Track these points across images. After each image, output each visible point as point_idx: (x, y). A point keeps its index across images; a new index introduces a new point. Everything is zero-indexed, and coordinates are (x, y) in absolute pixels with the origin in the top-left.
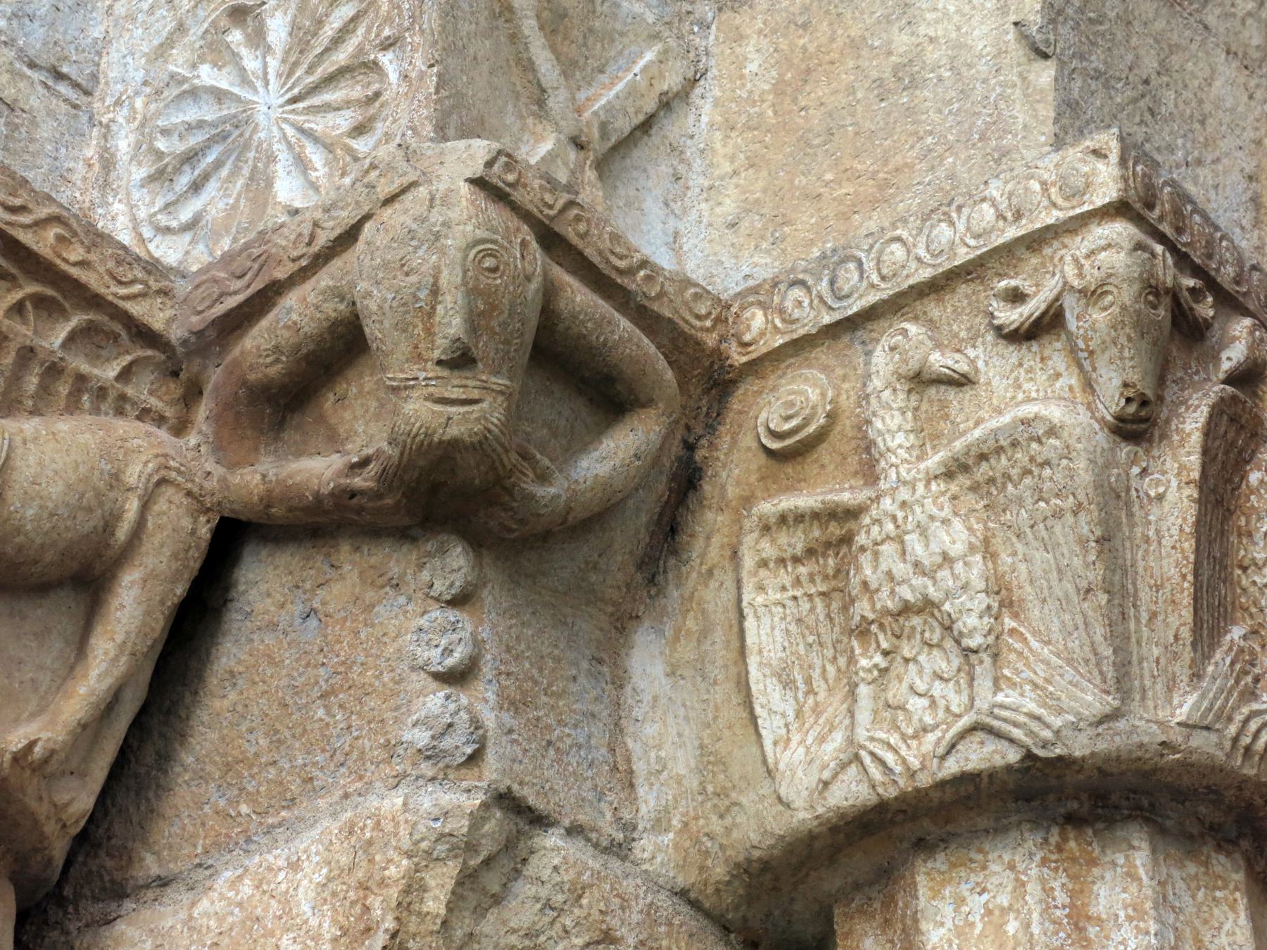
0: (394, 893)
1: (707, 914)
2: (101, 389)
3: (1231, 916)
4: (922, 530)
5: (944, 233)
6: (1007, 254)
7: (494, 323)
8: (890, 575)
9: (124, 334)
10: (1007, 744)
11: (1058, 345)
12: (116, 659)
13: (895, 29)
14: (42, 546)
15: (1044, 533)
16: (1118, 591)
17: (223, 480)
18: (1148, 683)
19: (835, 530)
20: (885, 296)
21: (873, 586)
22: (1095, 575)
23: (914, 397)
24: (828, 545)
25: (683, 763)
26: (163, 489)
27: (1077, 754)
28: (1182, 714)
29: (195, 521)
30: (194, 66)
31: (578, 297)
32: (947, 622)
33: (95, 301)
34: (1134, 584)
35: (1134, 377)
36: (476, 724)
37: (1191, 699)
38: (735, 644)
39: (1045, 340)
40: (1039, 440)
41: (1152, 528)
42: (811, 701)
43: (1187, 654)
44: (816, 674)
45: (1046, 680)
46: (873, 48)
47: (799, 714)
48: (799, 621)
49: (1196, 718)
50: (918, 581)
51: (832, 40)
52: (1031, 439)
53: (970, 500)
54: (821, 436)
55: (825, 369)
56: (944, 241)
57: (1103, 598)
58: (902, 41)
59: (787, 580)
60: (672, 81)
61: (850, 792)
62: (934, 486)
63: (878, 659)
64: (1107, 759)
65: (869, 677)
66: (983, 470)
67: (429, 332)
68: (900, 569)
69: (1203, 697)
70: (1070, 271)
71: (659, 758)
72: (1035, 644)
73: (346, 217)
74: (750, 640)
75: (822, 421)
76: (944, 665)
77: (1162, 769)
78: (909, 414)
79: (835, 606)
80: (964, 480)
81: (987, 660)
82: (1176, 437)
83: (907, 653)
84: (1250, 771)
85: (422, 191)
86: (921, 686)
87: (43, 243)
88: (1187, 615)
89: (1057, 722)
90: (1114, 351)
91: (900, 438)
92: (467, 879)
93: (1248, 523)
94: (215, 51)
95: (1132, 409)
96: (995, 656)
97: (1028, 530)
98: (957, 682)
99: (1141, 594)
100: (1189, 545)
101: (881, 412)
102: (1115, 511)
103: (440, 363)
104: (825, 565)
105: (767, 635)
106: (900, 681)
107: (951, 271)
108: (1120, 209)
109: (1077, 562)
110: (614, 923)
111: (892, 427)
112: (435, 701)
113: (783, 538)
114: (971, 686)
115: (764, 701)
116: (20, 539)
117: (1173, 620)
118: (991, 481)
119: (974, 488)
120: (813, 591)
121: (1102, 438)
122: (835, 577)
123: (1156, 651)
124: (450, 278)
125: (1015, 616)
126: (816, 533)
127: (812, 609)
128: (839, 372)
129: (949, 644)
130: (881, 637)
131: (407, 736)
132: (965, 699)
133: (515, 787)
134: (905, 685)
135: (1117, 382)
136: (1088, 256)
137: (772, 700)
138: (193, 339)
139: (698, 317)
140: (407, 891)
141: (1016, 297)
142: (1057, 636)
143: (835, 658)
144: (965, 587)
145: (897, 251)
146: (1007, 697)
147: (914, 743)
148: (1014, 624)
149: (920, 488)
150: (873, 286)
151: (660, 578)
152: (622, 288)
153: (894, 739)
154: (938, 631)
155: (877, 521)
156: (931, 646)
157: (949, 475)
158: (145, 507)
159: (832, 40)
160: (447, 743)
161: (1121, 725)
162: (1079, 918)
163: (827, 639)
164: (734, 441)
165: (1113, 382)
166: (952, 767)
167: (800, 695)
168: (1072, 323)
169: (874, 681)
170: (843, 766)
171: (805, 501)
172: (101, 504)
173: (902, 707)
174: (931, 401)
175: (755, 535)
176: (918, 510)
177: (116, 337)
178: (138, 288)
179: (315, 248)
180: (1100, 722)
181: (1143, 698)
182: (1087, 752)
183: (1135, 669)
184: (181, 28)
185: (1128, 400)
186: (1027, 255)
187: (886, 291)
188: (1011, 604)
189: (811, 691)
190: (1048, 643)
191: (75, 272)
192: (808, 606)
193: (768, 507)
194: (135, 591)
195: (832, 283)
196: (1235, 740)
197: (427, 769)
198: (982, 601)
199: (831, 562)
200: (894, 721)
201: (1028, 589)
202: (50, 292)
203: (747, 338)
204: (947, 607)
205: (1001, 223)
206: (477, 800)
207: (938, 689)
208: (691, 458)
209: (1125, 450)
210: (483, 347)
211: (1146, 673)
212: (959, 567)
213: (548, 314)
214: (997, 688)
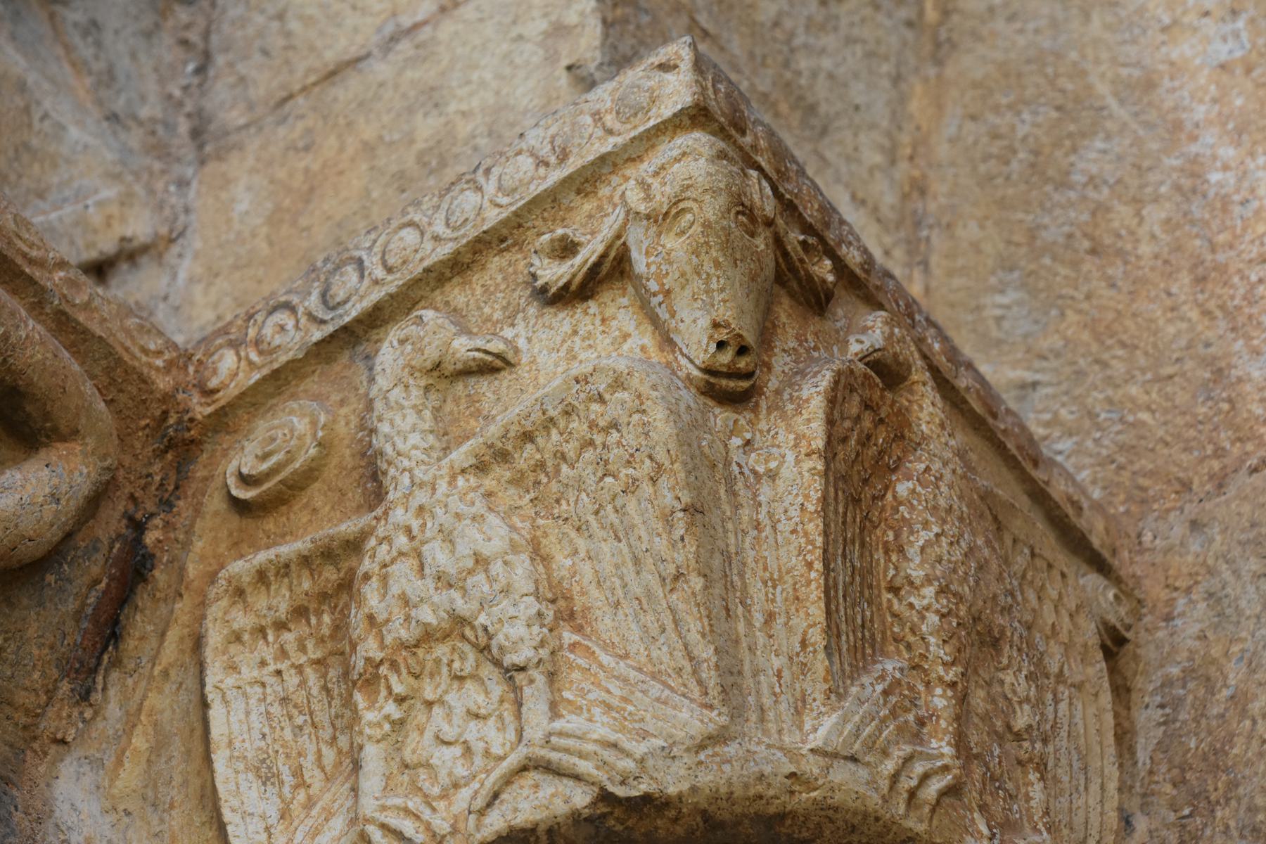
4: (448, 537)
5: (469, 200)
6: (550, 202)
8: (405, 601)
10: (571, 783)
11: (624, 301)
13: (419, 116)
15: (613, 517)
16: (721, 582)
18: (767, 701)
19: (330, 575)
20: (392, 289)
21: (381, 618)
22: (685, 555)
23: (433, 396)
24: (324, 597)
27: (672, 790)
28: (816, 740)
32: (483, 640)
34: (741, 575)
35: (725, 313)
37: (829, 722)
38: (198, 748)
39: (606, 296)
40: (601, 399)
41: (764, 510)
42: (301, 796)
43: (820, 663)
44: (308, 762)
45: (625, 700)
46: (391, 143)
47: (284, 815)
48: (285, 700)
49: (837, 743)
50: (442, 598)
51: (342, 149)
52: (591, 400)
53: (510, 496)
54: (310, 474)
55: (317, 397)
56: (468, 207)
57: (697, 583)
58: (426, 127)
59: (267, 652)
60: (140, 227)
62: (461, 482)
63: (391, 709)
64: (715, 798)
65: (378, 733)
69: (845, 720)
70: (634, 197)
72: (605, 659)
74: (216, 731)
75: (313, 451)
76: (481, 699)
77: (793, 814)
78: (427, 414)
79: (333, 674)
80: (502, 472)
81: (540, 679)
82: (790, 407)
83: (429, 694)
84: (916, 825)
86: (449, 732)
88: (817, 611)
89: (640, 749)
90: (698, 284)
91: (415, 439)
93: (897, 537)
95: (726, 357)
96: (552, 676)
97: (591, 518)
98: (501, 717)
99: (751, 590)
100: (814, 528)
101: (390, 415)
102: (712, 500)
104: (319, 623)
105: (237, 722)
106: (421, 731)
107: (478, 240)
109: (661, 544)
111: (405, 429)
113: (260, 601)
114: (518, 715)
115: (235, 803)
117: (799, 622)
118: (541, 466)
119: (518, 481)
120: (303, 659)
121: (688, 397)
122: (332, 637)
123: (777, 663)
125: (579, 629)
126: (306, 585)
127: (303, 684)
128: (335, 397)
129: (487, 670)
130: (394, 679)
132: (511, 735)
134: (429, 735)
135: (704, 322)
136: (656, 174)
139: (145, 351)
141: (566, 249)
142: (637, 647)
143: (334, 738)
144: (506, 591)
145: (410, 236)
147: (441, 805)
148: (576, 638)
149: (443, 486)
150: (376, 282)
151: (96, 697)
152: (31, 281)
153: (414, 803)
154: (471, 656)
155: (387, 539)
156: (461, 679)
157: (481, 468)
159: (342, 149)
161: (731, 749)
163: (322, 717)
164: (198, 511)
167: (286, 790)
168: (640, 262)
169: (385, 737)
171: (288, 550)
173: (428, 765)
174: (457, 401)
175: (224, 603)
176: (439, 511)
180: (701, 747)
181: (762, 720)
182: (685, 786)
183: (749, 682)
185: (721, 345)
186: (577, 201)
187: (393, 283)
188: (572, 615)
190: (626, 656)
192: (296, 680)
193: (240, 568)
195: (324, 296)
196: (895, 778)
198: (530, 606)
199: (326, 618)
200: (413, 782)
201: (594, 592)
203: (213, 383)
204: (482, 619)
205: (542, 171)
207: (473, 731)
208: (138, 541)
209: (721, 417)
211: (765, 691)
212: (497, 568)
214: (554, 710)
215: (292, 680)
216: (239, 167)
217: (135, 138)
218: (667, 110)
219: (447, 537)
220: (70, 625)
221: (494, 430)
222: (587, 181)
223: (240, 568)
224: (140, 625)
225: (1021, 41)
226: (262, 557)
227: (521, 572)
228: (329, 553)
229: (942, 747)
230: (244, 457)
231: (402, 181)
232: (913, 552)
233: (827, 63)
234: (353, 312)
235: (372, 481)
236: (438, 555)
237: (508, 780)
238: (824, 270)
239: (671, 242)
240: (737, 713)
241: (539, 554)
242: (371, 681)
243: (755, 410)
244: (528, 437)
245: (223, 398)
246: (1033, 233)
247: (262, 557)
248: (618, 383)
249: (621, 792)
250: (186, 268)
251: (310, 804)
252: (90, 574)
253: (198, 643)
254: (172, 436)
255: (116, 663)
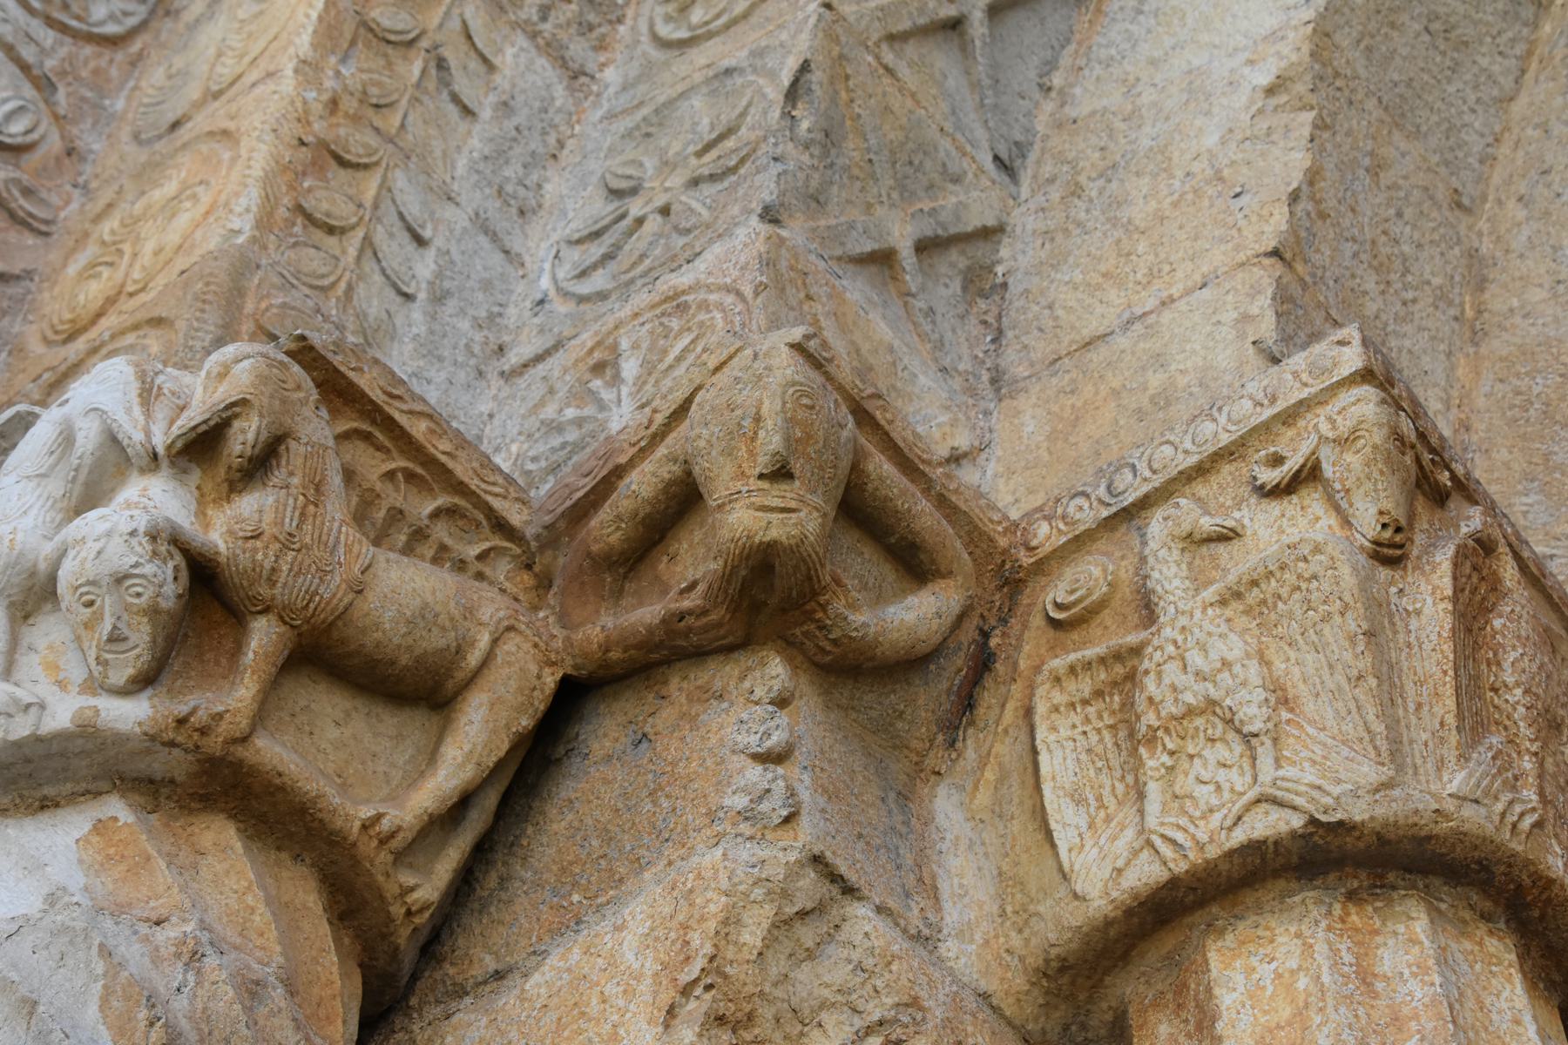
0: (712, 925)
1: (1009, 1023)
2: (462, 561)
3: (1508, 986)
4: (1204, 649)
5: (1208, 428)
6: (1264, 430)
7: (810, 450)
8: (1174, 689)
9: (485, 523)
10: (1290, 811)
11: (1316, 496)
12: (462, 766)
13: (1150, 373)
14: (399, 646)
15: (1314, 638)
16: (1388, 682)
17: (567, 639)
18: (1419, 762)
19: (1119, 670)
20: (1157, 484)
21: (1157, 699)
22: (1365, 664)
23: (1187, 555)
24: (1115, 684)
25: (982, 892)
26: (512, 634)
27: (1358, 818)
28: (1453, 788)
29: (541, 668)
30: (561, 410)
31: (881, 467)
32: (1228, 716)
33: (460, 488)
34: (1400, 677)
35: (1387, 505)
36: (791, 793)
37: (1460, 776)
38: (1030, 781)
39: (1304, 492)
40: (1305, 560)
41: (1413, 635)
42: (1102, 814)
43: (1454, 738)
44: (1106, 792)
45: (1324, 757)
46: (1132, 389)
48: (1089, 751)
49: (1465, 791)
50: (1200, 687)
51: (1097, 393)
52: (1298, 560)
54: (1102, 604)
55: (1105, 554)
56: (1207, 432)
57: (1373, 682)
58: (1155, 380)
59: (1077, 720)
61: (1146, 874)
62: (1210, 611)
63: (1165, 758)
64: (1386, 825)
65: (1157, 775)
66: (1254, 596)
67: (752, 453)
68: (1182, 680)
69: (1470, 775)
70: (1325, 428)
71: (961, 886)
72: (1311, 730)
73: (680, 396)
75: (1104, 589)
76: (1227, 754)
77: (1437, 837)
78: (1184, 566)
79: (1122, 734)
80: (1236, 605)
81: (1268, 743)
82: (1427, 568)
83: (1191, 750)
85: (748, 352)
86: (1206, 776)
87: (419, 429)
88: (1451, 703)
89: (1336, 791)
90: (1369, 486)
91: (1176, 582)
92: (782, 924)
93: (1495, 654)
94: (582, 394)
95: (1388, 534)
96: (1275, 740)
97: (1299, 637)
98: (1241, 767)
99: (1407, 688)
100: (1448, 648)
101: (1158, 566)
102: (1380, 630)
103: (761, 476)
104: (1112, 701)
105: (1060, 761)
106: (1187, 775)
107: (1215, 453)
108: (1365, 375)
109: (1348, 656)
110: (923, 994)
111: (1169, 575)
112: (755, 774)
113: (1071, 686)
114: (1254, 766)
115: (1058, 817)
116: (378, 635)
118: (1264, 602)
119: (1248, 612)
120: (1101, 725)
121: (1362, 559)
122: (1121, 710)
123: (1424, 736)
124: (770, 407)
125: (1292, 710)
126: (1103, 676)
127: (1101, 740)
128: (1118, 554)
129: (1231, 735)
130: (1167, 740)
131: (727, 802)
132: (1248, 779)
133: (828, 854)
134: (1191, 777)
135: (1373, 511)
136: (1339, 413)
137: (1066, 819)
138: (545, 533)
139: (991, 521)
140: (726, 922)
141: (1277, 460)
143: (1123, 777)
144: (1244, 684)
145: (1168, 450)
146: (1288, 771)
147: (1201, 823)
148: (1290, 716)
149: (1198, 614)
150: (1145, 480)
151: (959, 745)
152: (924, 474)
153: (1183, 821)
154: (1220, 726)
155: (1161, 648)
156: (1213, 741)
157: (1223, 602)
158: (495, 642)
159: (1097, 393)
160: (765, 806)
161: (1397, 792)
162: (1365, 977)
163: (1115, 763)
164: (1025, 626)
165: (1367, 518)
166: (1239, 837)
167: (1092, 809)
168: (1328, 470)
169: (1162, 777)
170: (1135, 853)
171: (1090, 653)
172: (455, 628)
173: (1191, 797)
174: (1203, 559)
175: (1047, 686)
176: (1196, 630)
177: (478, 525)
178: (497, 490)
179: (653, 428)
180: (1377, 790)
181: (1416, 774)
182: (1366, 816)
183: (1407, 749)
184: (552, 391)
185: (1384, 526)
186: (1283, 429)
187: (1158, 481)
188: (1286, 701)
189: (1102, 806)
190: (1324, 729)
191: (443, 458)
192: (1096, 738)
193: (1058, 663)
194: (483, 711)
195: (1109, 487)
196: (1503, 815)
197: (745, 828)
198: (1260, 695)
199: (1116, 698)
200: (1182, 808)
201: (1301, 686)
202: (419, 470)
203: (1034, 543)
204: (1228, 702)
205: (1258, 409)
206: (793, 856)
207: (1222, 775)
208: (986, 644)
209: (1384, 573)
210: (797, 466)
211: (1417, 755)
212: (1237, 669)
213: (856, 468)
214: (1278, 766)
215: (1094, 738)
216: (1025, 403)
217: (957, 383)
218: (1345, 371)
219: (1199, 649)
220: (944, 697)
221: (1231, 578)
222: (1289, 417)
223: (1058, 663)
224: (987, 699)
225: (1533, 331)
226: (1072, 657)
227: (1253, 671)
228: (1118, 656)
229: (1530, 795)
230: (1058, 591)
231: (1140, 415)
232: (1506, 665)
233: (1407, 343)
234: (1129, 498)
235: (1147, 609)
236: (1195, 659)
237: (1247, 809)
238: (1444, 478)
239: (1349, 457)
240: (1400, 768)
241: (1265, 662)
242: (1151, 740)
243: (1405, 569)
244: (1255, 583)
245: (1041, 553)
246: (1547, 457)
247: (1072, 657)
248: (1317, 549)
249: (1323, 818)
250: (991, 468)
251: (1108, 819)
252: (957, 664)
253: (1029, 712)
254: (1009, 578)
255: (972, 723)
